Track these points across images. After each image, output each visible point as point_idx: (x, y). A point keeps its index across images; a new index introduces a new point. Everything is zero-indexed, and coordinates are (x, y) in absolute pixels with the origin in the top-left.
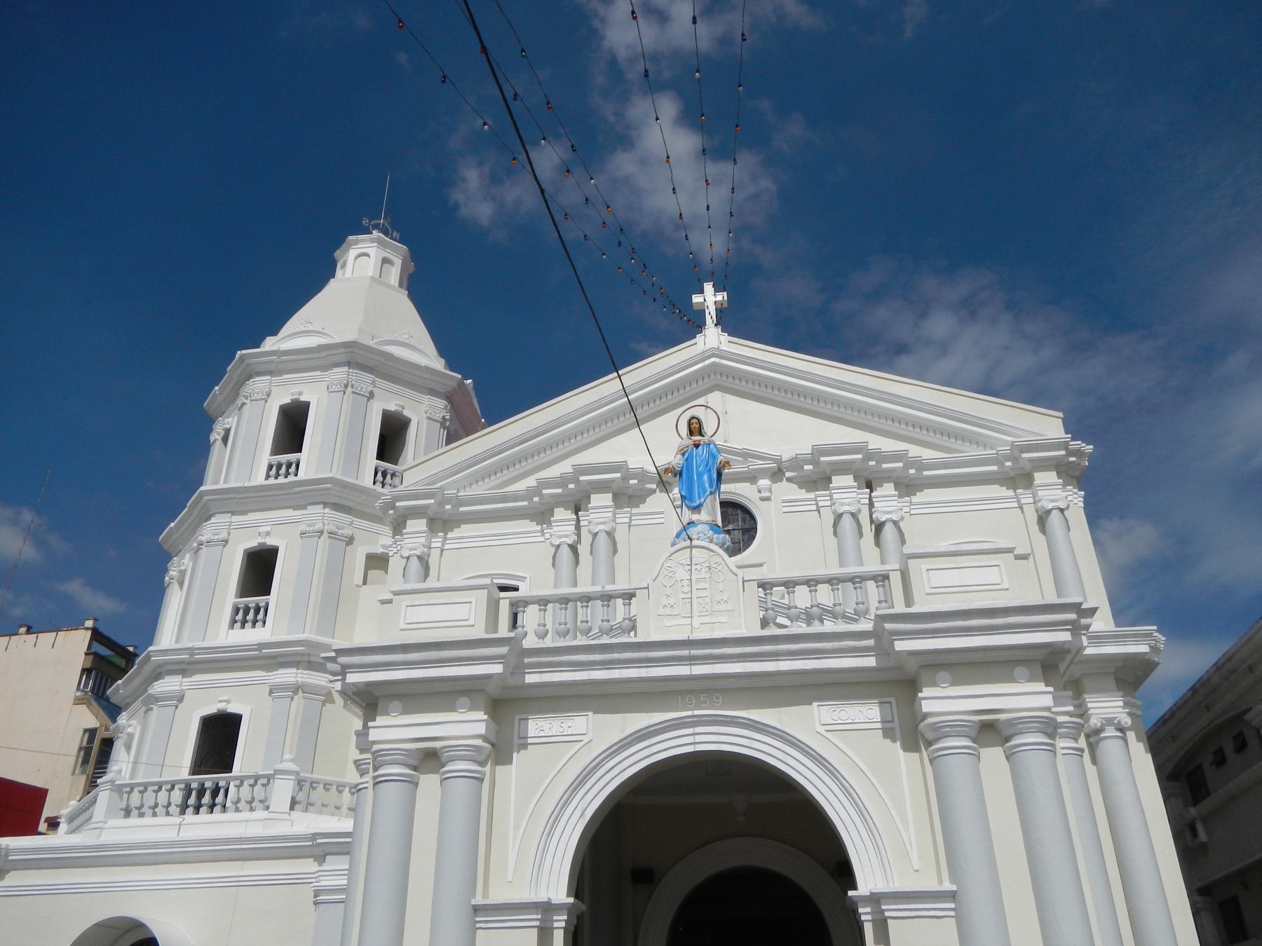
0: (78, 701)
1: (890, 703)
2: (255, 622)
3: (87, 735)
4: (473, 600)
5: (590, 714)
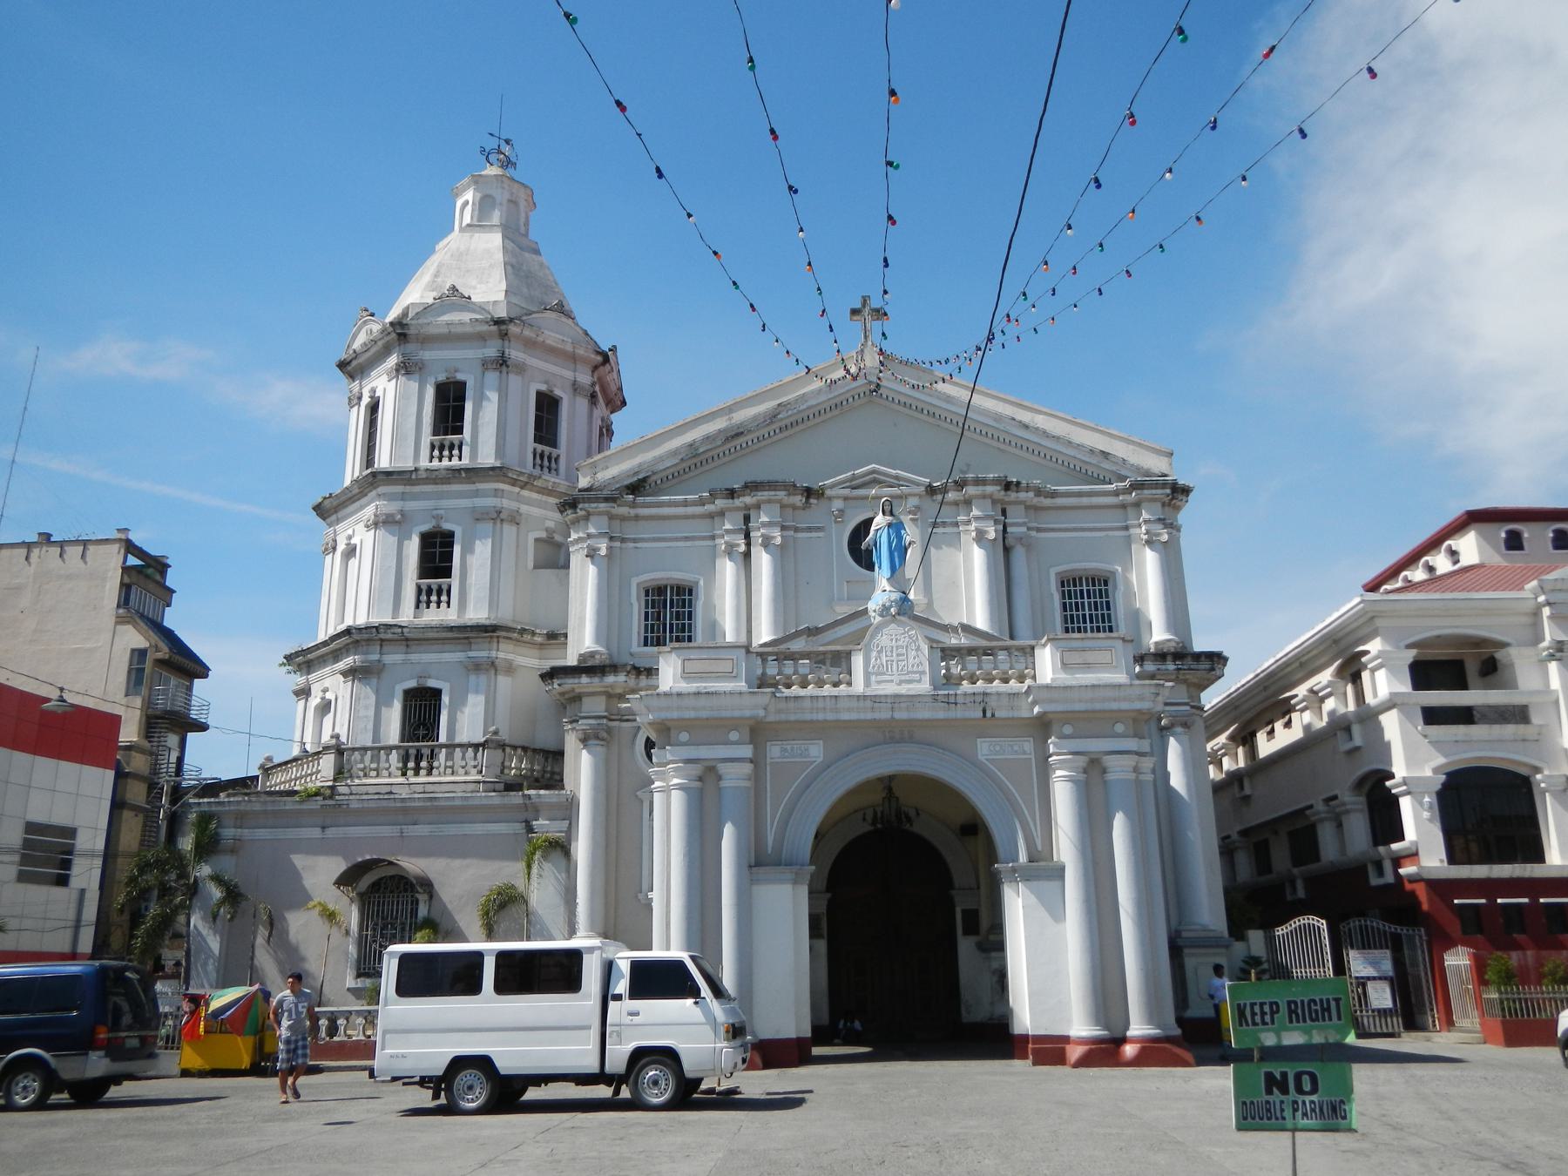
0: (120, 620)
1: (1029, 741)
2: (439, 603)
3: (136, 653)
4: (735, 657)
5: (821, 742)
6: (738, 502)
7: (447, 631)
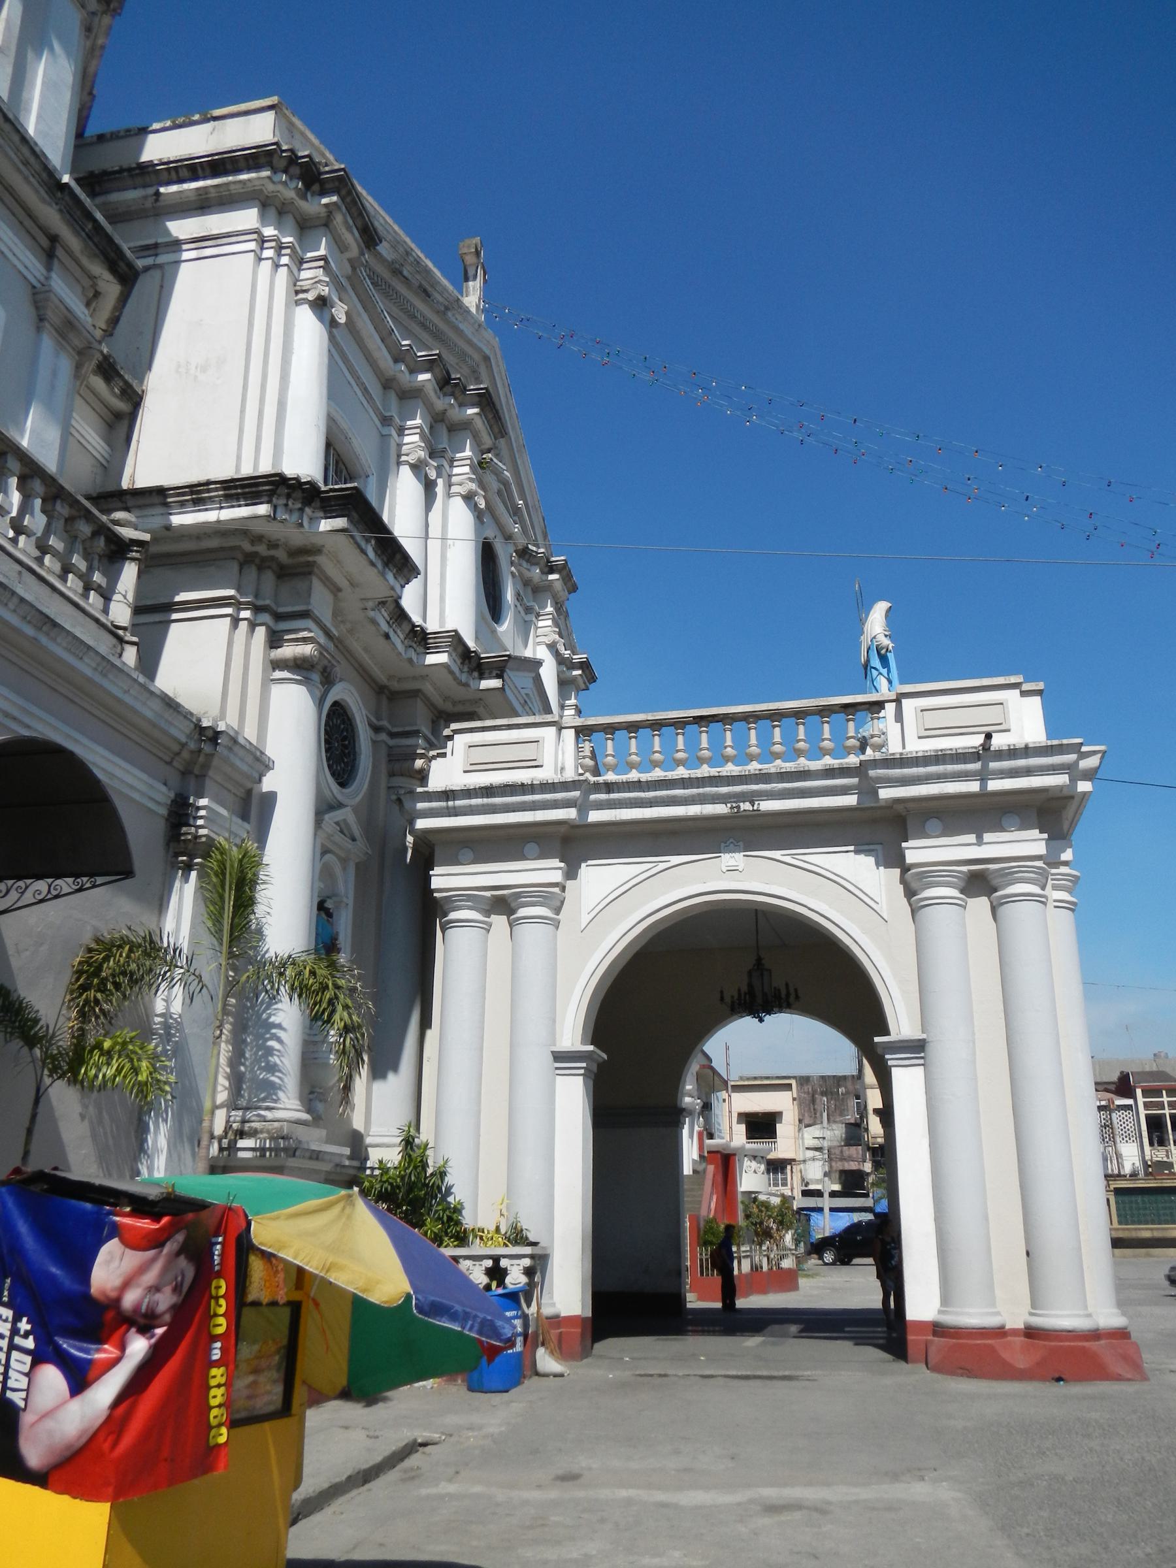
6: (442, 403)
7: (43, 183)
